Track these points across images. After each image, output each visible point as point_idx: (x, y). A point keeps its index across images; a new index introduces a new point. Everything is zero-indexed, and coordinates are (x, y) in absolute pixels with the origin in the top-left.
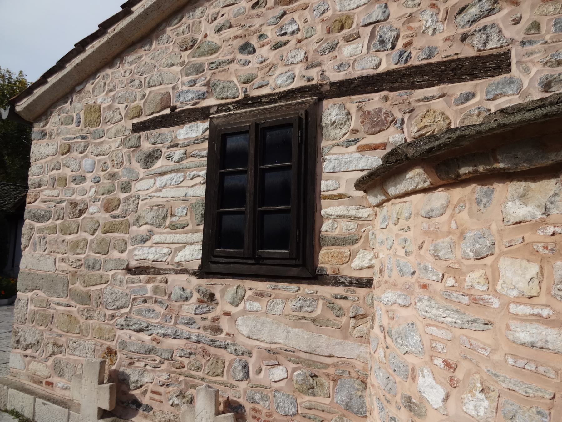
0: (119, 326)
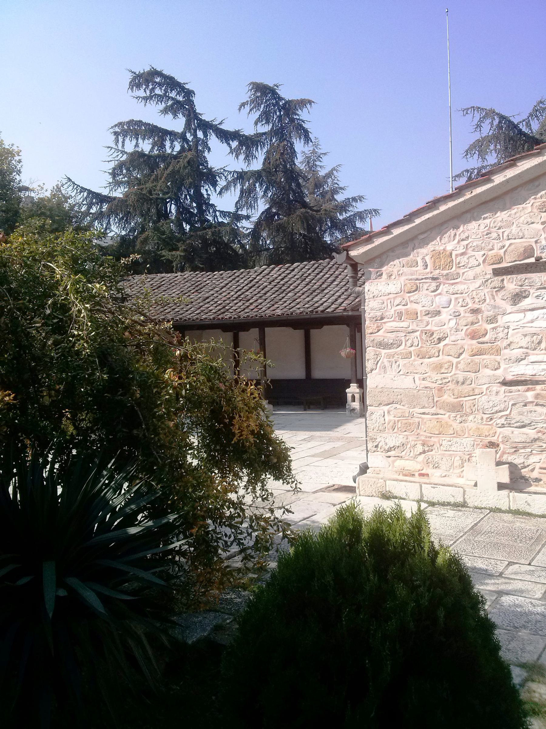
0: (500, 425)
